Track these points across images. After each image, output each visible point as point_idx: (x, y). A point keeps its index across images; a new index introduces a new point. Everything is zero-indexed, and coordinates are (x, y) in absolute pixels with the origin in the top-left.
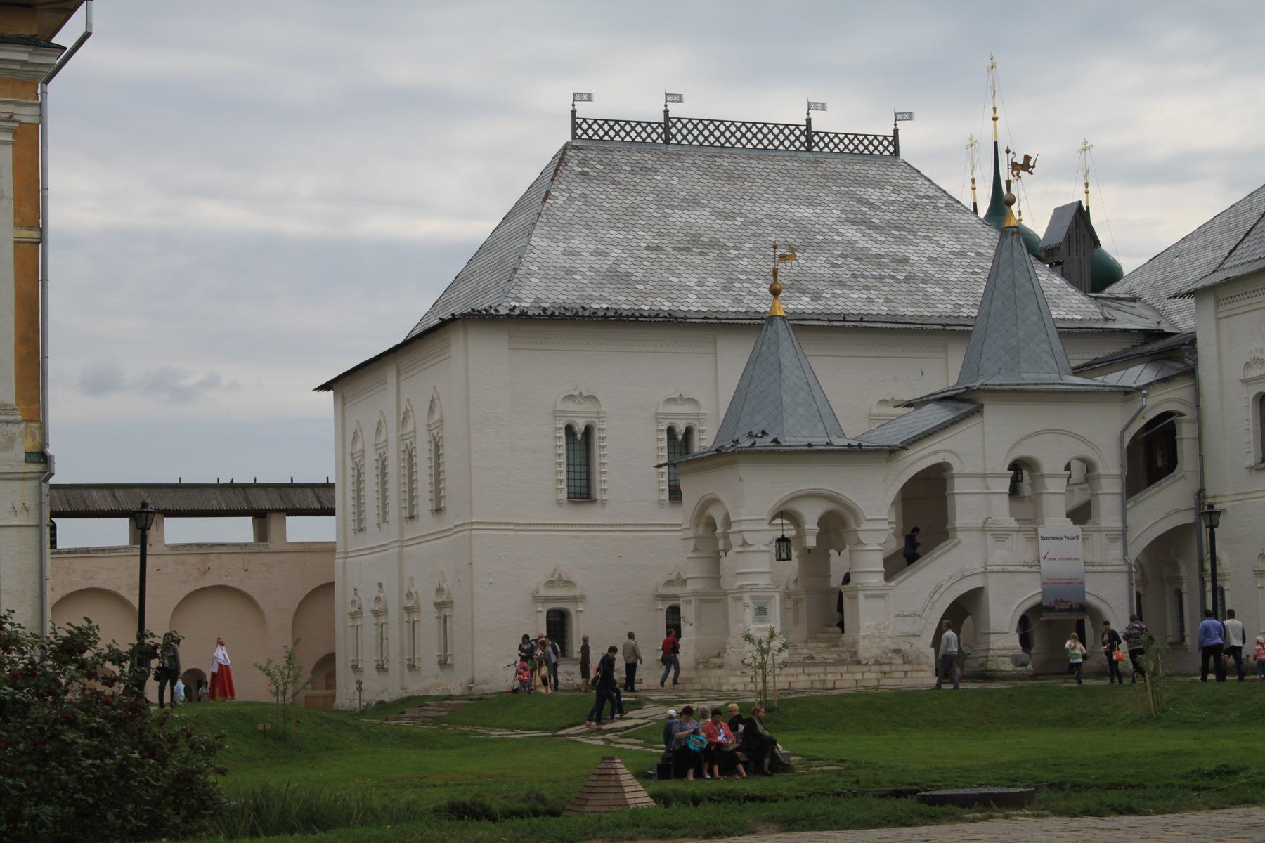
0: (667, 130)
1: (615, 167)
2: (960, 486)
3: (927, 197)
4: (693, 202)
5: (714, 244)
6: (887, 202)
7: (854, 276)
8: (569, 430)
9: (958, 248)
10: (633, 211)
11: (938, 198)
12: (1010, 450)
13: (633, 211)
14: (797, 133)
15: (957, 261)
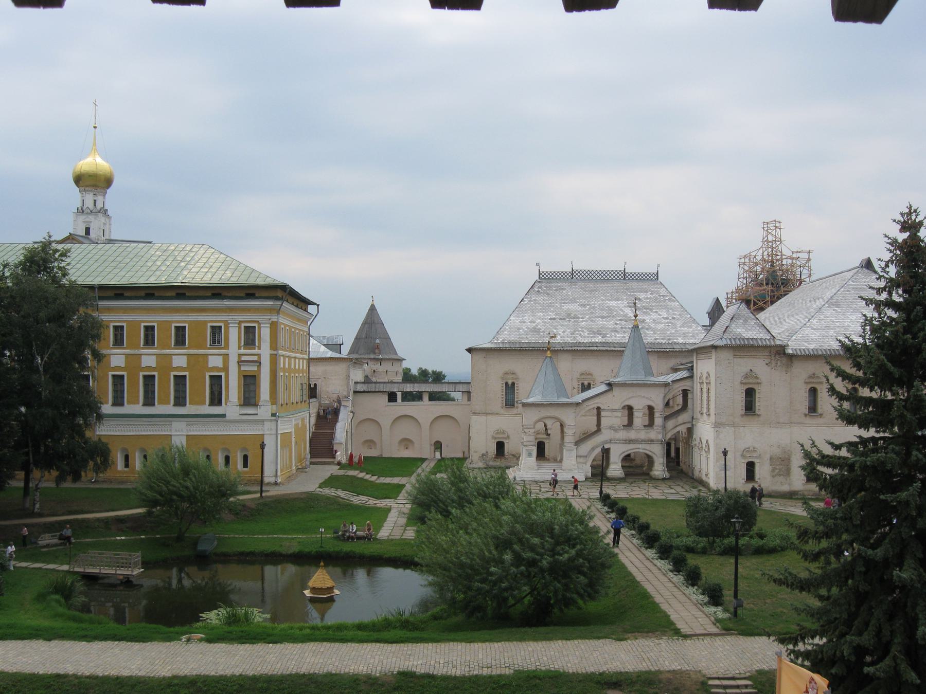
0: (572, 274)
1: (550, 288)
2: (603, 414)
3: (663, 296)
4: (574, 301)
5: (576, 317)
6: (647, 298)
7: (622, 328)
8: (507, 384)
9: (666, 315)
10: (550, 305)
11: (667, 296)
12: (622, 403)
13: (550, 305)
14: (620, 273)
15: (664, 321)
